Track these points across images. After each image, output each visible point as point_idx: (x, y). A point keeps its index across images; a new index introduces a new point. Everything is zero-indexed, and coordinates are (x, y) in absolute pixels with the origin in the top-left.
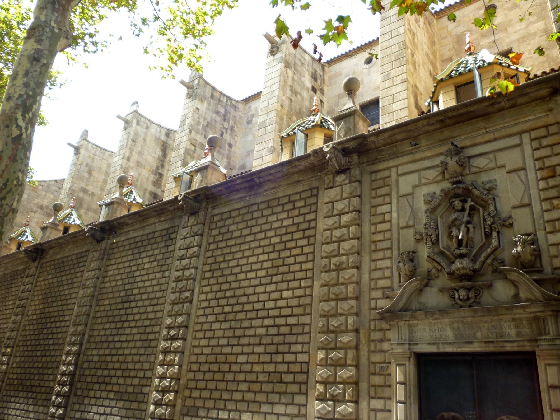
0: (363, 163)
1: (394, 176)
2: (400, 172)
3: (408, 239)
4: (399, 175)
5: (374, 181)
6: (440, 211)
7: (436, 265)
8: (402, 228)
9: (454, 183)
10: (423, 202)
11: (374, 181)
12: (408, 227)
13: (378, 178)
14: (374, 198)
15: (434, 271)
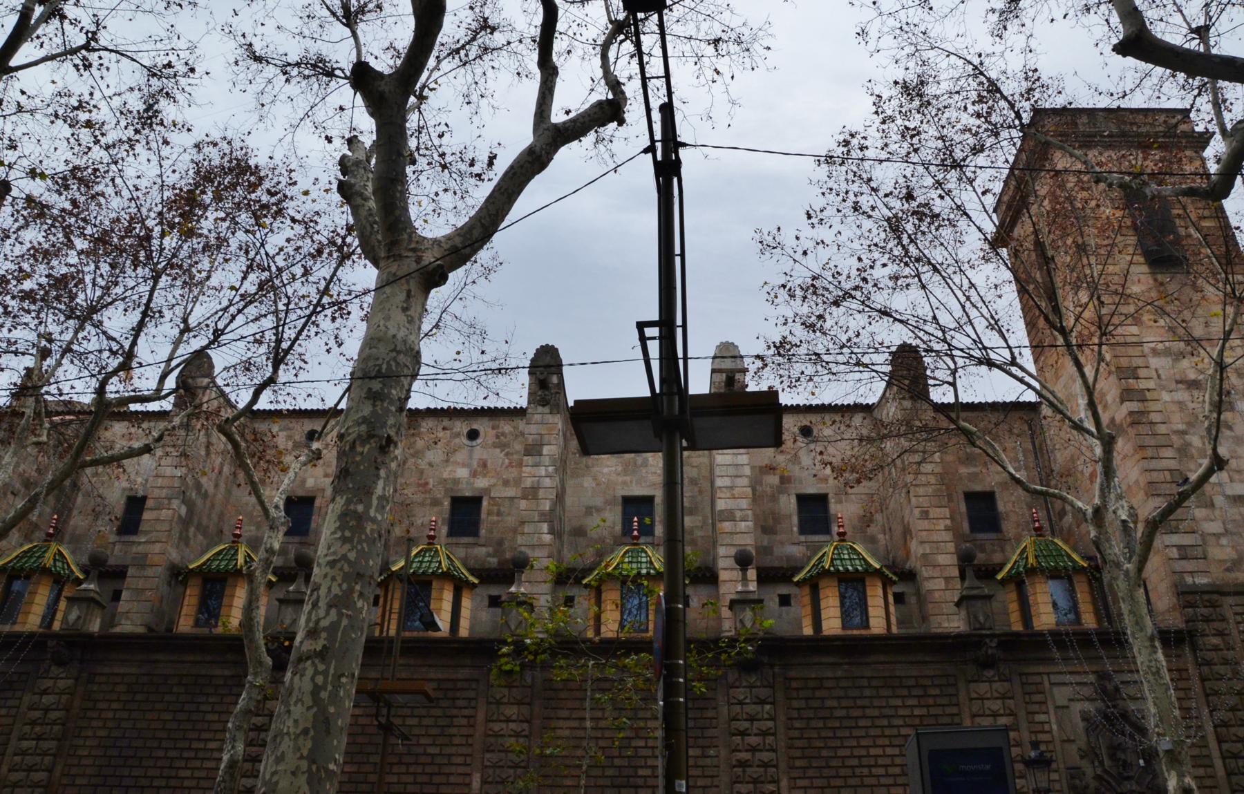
1: (1047, 684)
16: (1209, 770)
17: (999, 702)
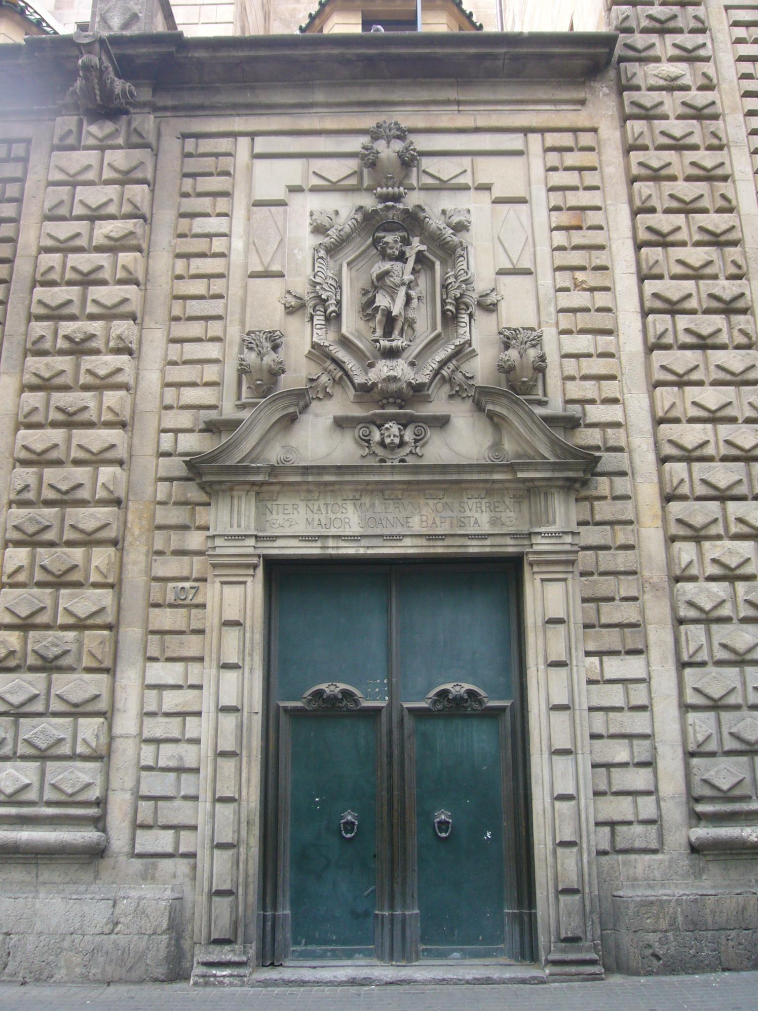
0: (165, 109)
2: (257, 150)
3: (267, 306)
5: (189, 155)
6: (350, 253)
7: (332, 367)
8: (254, 275)
9: (383, 198)
10: (308, 229)
11: (189, 155)
12: (267, 274)
13: (201, 150)
15: (324, 379)
16: (602, 339)
17: (112, 191)
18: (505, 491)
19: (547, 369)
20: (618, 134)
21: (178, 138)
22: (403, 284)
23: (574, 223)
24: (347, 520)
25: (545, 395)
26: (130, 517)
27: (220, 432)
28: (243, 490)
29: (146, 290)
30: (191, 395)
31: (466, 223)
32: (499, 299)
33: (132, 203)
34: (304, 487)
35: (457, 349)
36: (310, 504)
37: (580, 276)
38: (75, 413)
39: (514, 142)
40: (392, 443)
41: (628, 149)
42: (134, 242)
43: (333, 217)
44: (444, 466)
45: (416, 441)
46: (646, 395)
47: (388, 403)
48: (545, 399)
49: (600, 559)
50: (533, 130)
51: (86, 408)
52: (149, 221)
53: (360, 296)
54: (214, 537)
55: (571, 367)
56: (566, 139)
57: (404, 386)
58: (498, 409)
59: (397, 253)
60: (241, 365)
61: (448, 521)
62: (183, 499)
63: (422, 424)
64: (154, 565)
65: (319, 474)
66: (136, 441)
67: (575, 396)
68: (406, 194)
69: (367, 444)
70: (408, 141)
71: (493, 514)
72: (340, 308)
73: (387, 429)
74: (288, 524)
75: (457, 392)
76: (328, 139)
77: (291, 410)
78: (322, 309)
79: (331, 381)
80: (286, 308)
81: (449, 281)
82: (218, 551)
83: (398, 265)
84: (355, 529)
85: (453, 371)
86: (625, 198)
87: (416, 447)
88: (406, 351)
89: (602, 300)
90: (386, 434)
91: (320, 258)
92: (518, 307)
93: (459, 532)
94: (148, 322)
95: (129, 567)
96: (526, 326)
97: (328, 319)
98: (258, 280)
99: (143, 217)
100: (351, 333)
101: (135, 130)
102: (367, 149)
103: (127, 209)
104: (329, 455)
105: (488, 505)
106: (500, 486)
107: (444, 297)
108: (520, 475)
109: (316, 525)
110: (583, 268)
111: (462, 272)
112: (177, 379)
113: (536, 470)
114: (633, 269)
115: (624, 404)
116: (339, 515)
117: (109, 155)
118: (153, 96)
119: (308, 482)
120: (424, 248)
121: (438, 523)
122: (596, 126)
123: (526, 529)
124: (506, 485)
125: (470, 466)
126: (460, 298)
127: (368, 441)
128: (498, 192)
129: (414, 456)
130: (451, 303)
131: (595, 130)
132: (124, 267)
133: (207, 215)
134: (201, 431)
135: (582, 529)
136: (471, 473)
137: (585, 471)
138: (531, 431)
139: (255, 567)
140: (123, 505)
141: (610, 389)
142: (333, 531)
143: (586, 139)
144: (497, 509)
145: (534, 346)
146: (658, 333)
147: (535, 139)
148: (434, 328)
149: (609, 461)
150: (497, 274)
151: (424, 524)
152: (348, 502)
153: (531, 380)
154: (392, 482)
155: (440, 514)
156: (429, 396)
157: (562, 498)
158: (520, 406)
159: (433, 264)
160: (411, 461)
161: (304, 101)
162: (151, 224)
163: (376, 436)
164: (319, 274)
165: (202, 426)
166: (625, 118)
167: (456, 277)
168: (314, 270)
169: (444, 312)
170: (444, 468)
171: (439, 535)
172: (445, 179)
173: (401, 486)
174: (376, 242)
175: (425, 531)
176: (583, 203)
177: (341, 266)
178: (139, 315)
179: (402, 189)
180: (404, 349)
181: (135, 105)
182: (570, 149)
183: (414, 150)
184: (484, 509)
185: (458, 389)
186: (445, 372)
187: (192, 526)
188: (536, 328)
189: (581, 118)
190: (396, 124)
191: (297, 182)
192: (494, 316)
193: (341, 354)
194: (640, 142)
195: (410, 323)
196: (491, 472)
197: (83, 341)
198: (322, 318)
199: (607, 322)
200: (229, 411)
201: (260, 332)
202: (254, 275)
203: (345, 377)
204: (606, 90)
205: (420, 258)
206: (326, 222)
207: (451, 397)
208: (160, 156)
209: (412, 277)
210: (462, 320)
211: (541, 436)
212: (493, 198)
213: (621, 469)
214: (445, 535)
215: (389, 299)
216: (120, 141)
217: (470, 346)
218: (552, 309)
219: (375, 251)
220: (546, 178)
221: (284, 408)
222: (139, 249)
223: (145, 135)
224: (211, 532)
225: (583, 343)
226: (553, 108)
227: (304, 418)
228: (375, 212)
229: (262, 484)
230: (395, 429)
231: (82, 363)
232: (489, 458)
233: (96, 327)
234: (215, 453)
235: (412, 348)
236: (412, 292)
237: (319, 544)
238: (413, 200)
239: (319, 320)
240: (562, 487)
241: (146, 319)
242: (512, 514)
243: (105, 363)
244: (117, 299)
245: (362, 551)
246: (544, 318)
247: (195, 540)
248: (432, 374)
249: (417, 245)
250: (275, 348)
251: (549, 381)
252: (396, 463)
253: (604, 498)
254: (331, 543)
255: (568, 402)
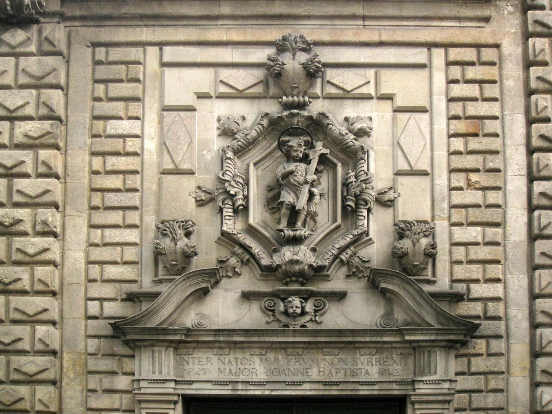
2: (166, 59)
3: (182, 200)
4: (164, 65)
5: (100, 63)
6: (255, 154)
7: (240, 251)
9: (287, 106)
10: (216, 133)
11: (100, 63)
13: (111, 59)
14: (99, 100)
16: (490, 231)
18: (394, 350)
19: (437, 255)
20: (519, 50)
21: (88, 47)
22: (306, 182)
23: (471, 130)
24: (254, 370)
25: (434, 275)
26: (65, 364)
27: (141, 301)
28: (162, 346)
29: (66, 183)
30: (112, 271)
31: (368, 130)
32: (396, 196)
33: (48, 106)
34: (217, 345)
35: (356, 238)
36: (222, 358)
37: (474, 177)
38: (10, 283)
39: (419, 56)
40: (294, 312)
41: (528, 64)
42: (52, 141)
43: (240, 122)
44: (339, 331)
45: (316, 311)
46: (526, 276)
47: (291, 281)
48: (434, 279)
49: (473, 399)
50: (437, 45)
51: (19, 280)
52: (64, 123)
53: (265, 192)
54: (139, 380)
55: (460, 253)
56: (470, 54)
57: (306, 267)
58: (390, 287)
59: (301, 155)
60: (157, 248)
61: (342, 372)
62: (110, 352)
63: (320, 298)
64: (89, 399)
65: (229, 335)
66: (66, 307)
67: (461, 277)
68: (310, 102)
69: (271, 313)
70: (313, 53)
71: (382, 367)
72: (247, 202)
73: (290, 301)
74: (203, 372)
75: (354, 273)
76: (234, 50)
77: (204, 285)
78: (230, 203)
79: (240, 263)
80: (197, 201)
81: (350, 180)
82: (143, 391)
83: (302, 166)
84: (262, 377)
85: (351, 256)
86: (522, 109)
87: (316, 316)
88: (308, 239)
89: (493, 197)
90: (290, 306)
91: (228, 158)
92: (414, 203)
93: (351, 380)
94: (69, 210)
95: (68, 401)
96: (420, 219)
97: (236, 211)
98: (170, 177)
99: (59, 119)
100: (258, 224)
101: (46, 39)
102: (273, 61)
103: (43, 111)
104: (238, 321)
105: (377, 360)
106: (390, 346)
107: (345, 194)
108: (407, 338)
109: (227, 374)
110: (477, 171)
111: (363, 172)
112: (99, 258)
113: (422, 334)
114: (524, 172)
115: (505, 283)
116: (247, 367)
117: (24, 62)
118: (62, 7)
119: (220, 342)
120: (327, 151)
121: (334, 373)
122: (499, 42)
123: (410, 377)
124: (395, 345)
125: (364, 331)
126: (359, 195)
127: (273, 311)
128: (400, 102)
129: (314, 323)
130: (351, 200)
131: (497, 46)
132: (44, 163)
133: (120, 118)
134: (122, 300)
135: (458, 378)
136: (364, 336)
137: (465, 335)
138: (420, 305)
139: (175, 403)
140: (58, 355)
141: (494, 271)
142: (242, 378)
143: (488, 54)
144: (386, 363)
145: (426, 236)
146: (542, 226)
147: (438, 55)
148: (335, 220)
149: (487, 327)
150: (396, 174)
151: (322, 374)
152: (254, 357)
153: (422, 263)
154: (294, 342)
155: (336, 367)
156: (328, 276)
157: (443, 355)
158: (411, 285)
159: (335, 165)
160: (311, 326)
161: (210, 14)
162: (66, 125)
163: (281, 307)
164: (228, 173)
165: (124, 296)
166: (527, 36)
167: (356, 177)
168: (222, 169)
169: (344, 207)
170: (340, 332)
171: (334, 382)
172: (349, 89)
173: (302, 345)
174: (281, 145)
175: (322, 379)
176: (482, 113)
177: (248, 166)
178: (60, 204)
179: (306, 98)
180: (306, 238)
181: (45, 14)
182: (472, 64)
183: (319, 62)
184: (374, 363)
185: (355, 270)
186: (344, 257)
187: (120, 372)
188: (429, 221)
189: (485, 34)
190: (302, 37)
191: (204, 90)
192: (391, 210)
193: (249, 241)
194: (540, 58)
195: (313, 216)
196: (382, 336)
197: (11, 225)
198: (230, 210)
199: (496, 217)
200: (147, 284)
201: (173, 221)
202: (165, 172)
203: (251, 259)
204: (511, 9)
205: (323, 159)
206: (234, 127)
207: (348, 276)
208: (72, 63)
209: (315, 177)
210: (361, 214)
211: (428, 308)
212: (395, 107)
213: (497, 333)
214: (340, 382)
215: (293, 195)
216: (33, 48)
217: (368, 235)
218: (445, 205)
219: (280, 153)
220: (447, 89)
221: (196, 284)
222: (57, 147)
223: (56, 43)
224: (137, 377)
225: (473, 233)
226: (457, 24)
227: (214, 291)
228: (280, 118)
229: (180, 342)
230: (297, 302)
231: (13, 244)
232: (381, 325)
233: (24, 213)
234: (137, 318)
235: (314, 236)
236: (315, 190)
237: (230, 387)
238: (316, 108)
239: (228, 211)
240: (444, 347)
241: (68, 208)
242: (399, 367)
243: (34, 244)
244: (40, 191)
245: (267, 393)
246: (437, 213)
247: (122, 382)
248: (331, 258)
249: (320, 148)
250: (188, 235)
251: (438, 265)
252: (298, 328)
253: (481, 355)
254: (240, 386)
255: (453, 281)
